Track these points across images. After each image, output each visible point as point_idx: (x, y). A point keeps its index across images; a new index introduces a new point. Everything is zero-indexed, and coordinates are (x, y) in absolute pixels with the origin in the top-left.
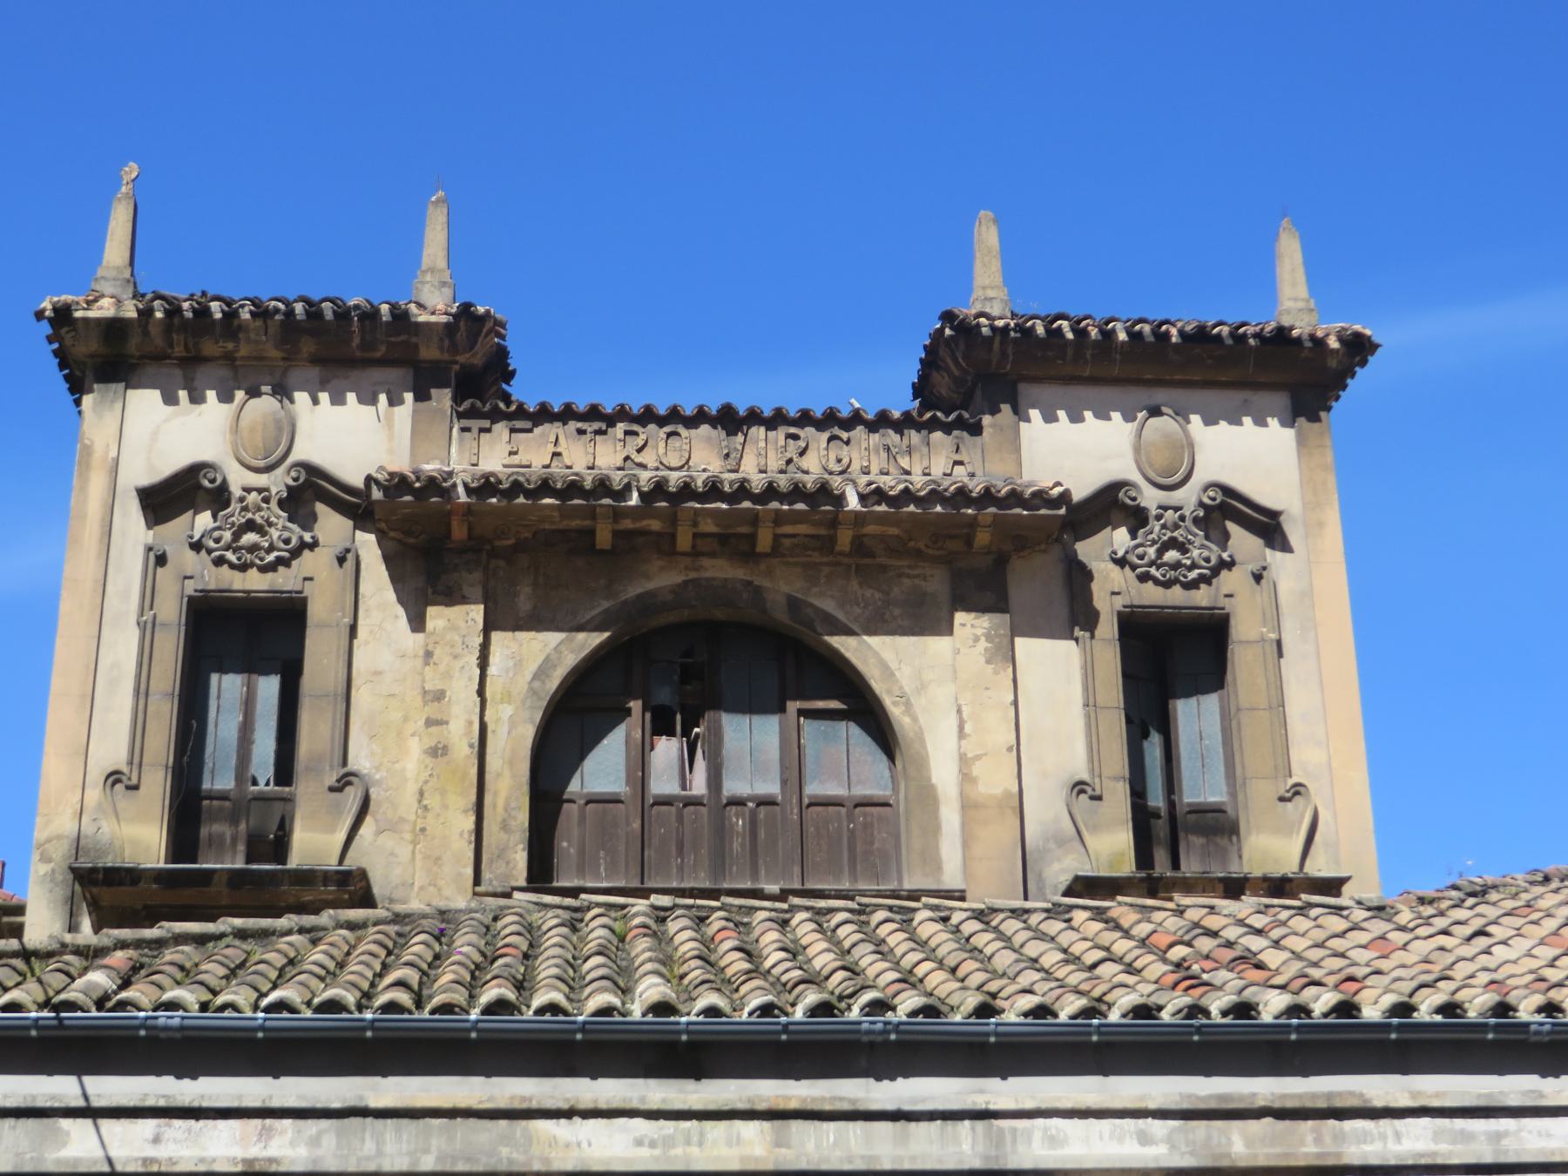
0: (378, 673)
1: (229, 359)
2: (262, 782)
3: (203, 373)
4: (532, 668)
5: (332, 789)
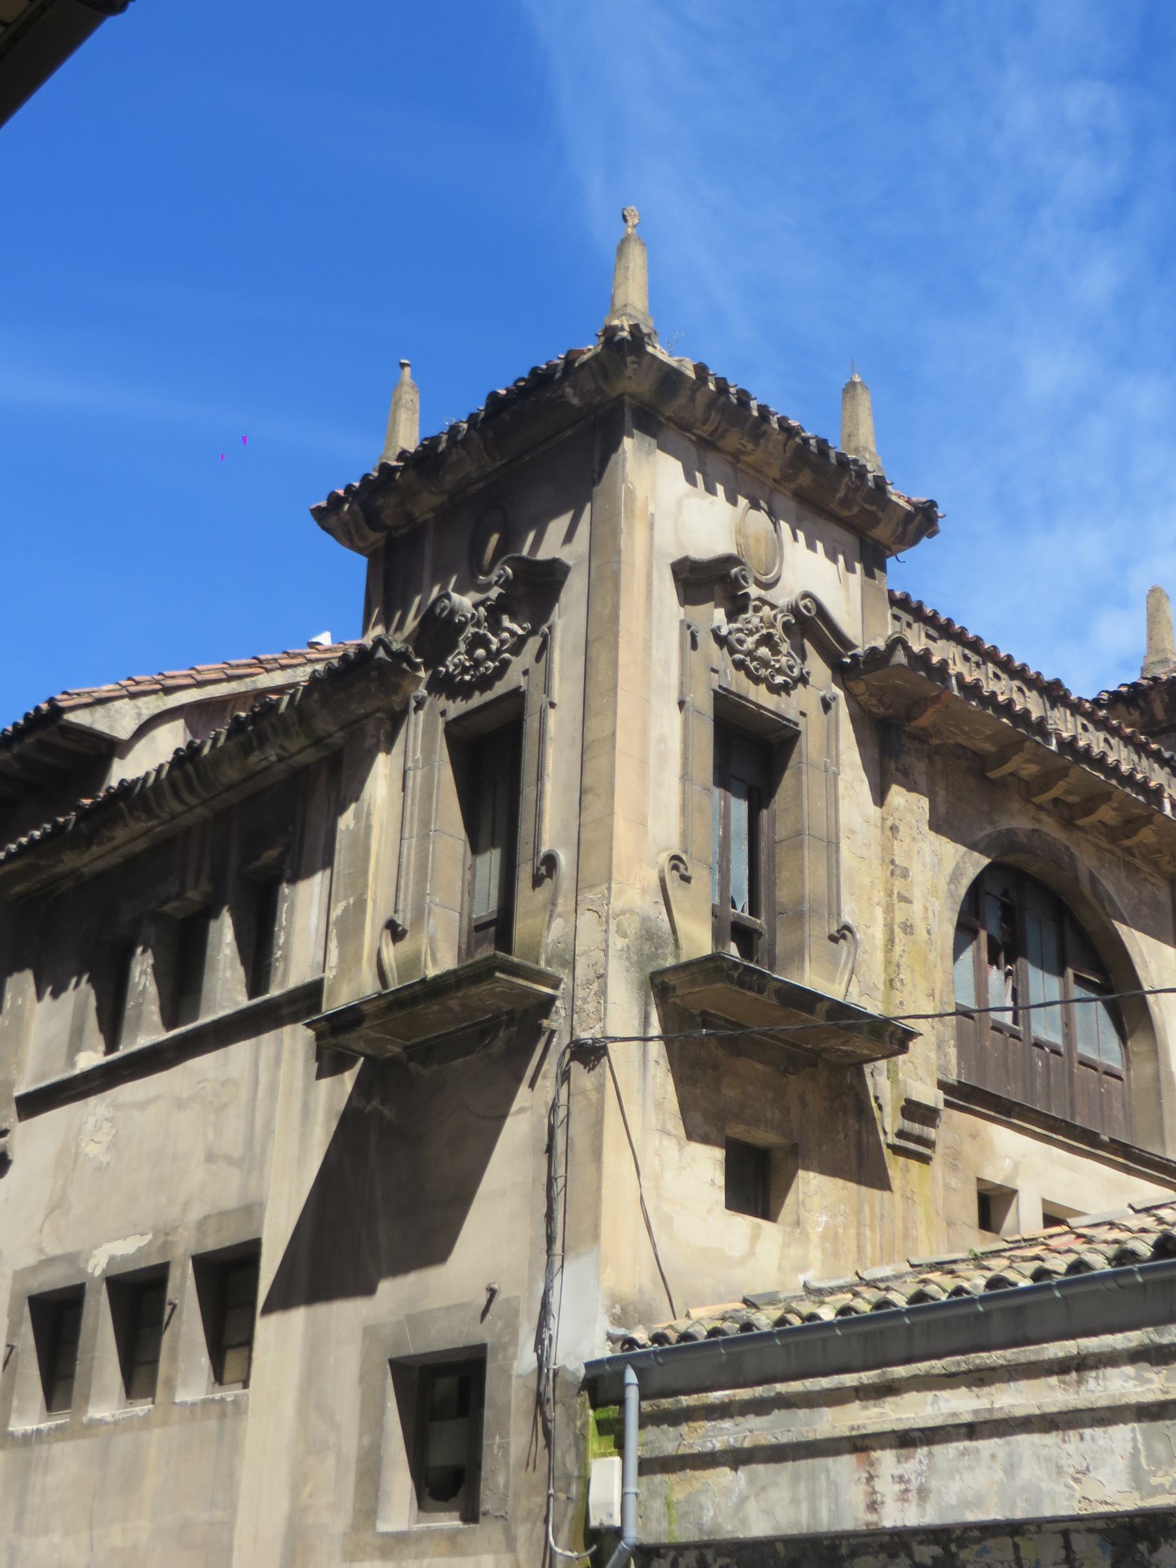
0: (853, 832)
1: (736, 456)
2: (739, 907)
3: (712, 458)
4: (949, 868)
5: (833, 939)
